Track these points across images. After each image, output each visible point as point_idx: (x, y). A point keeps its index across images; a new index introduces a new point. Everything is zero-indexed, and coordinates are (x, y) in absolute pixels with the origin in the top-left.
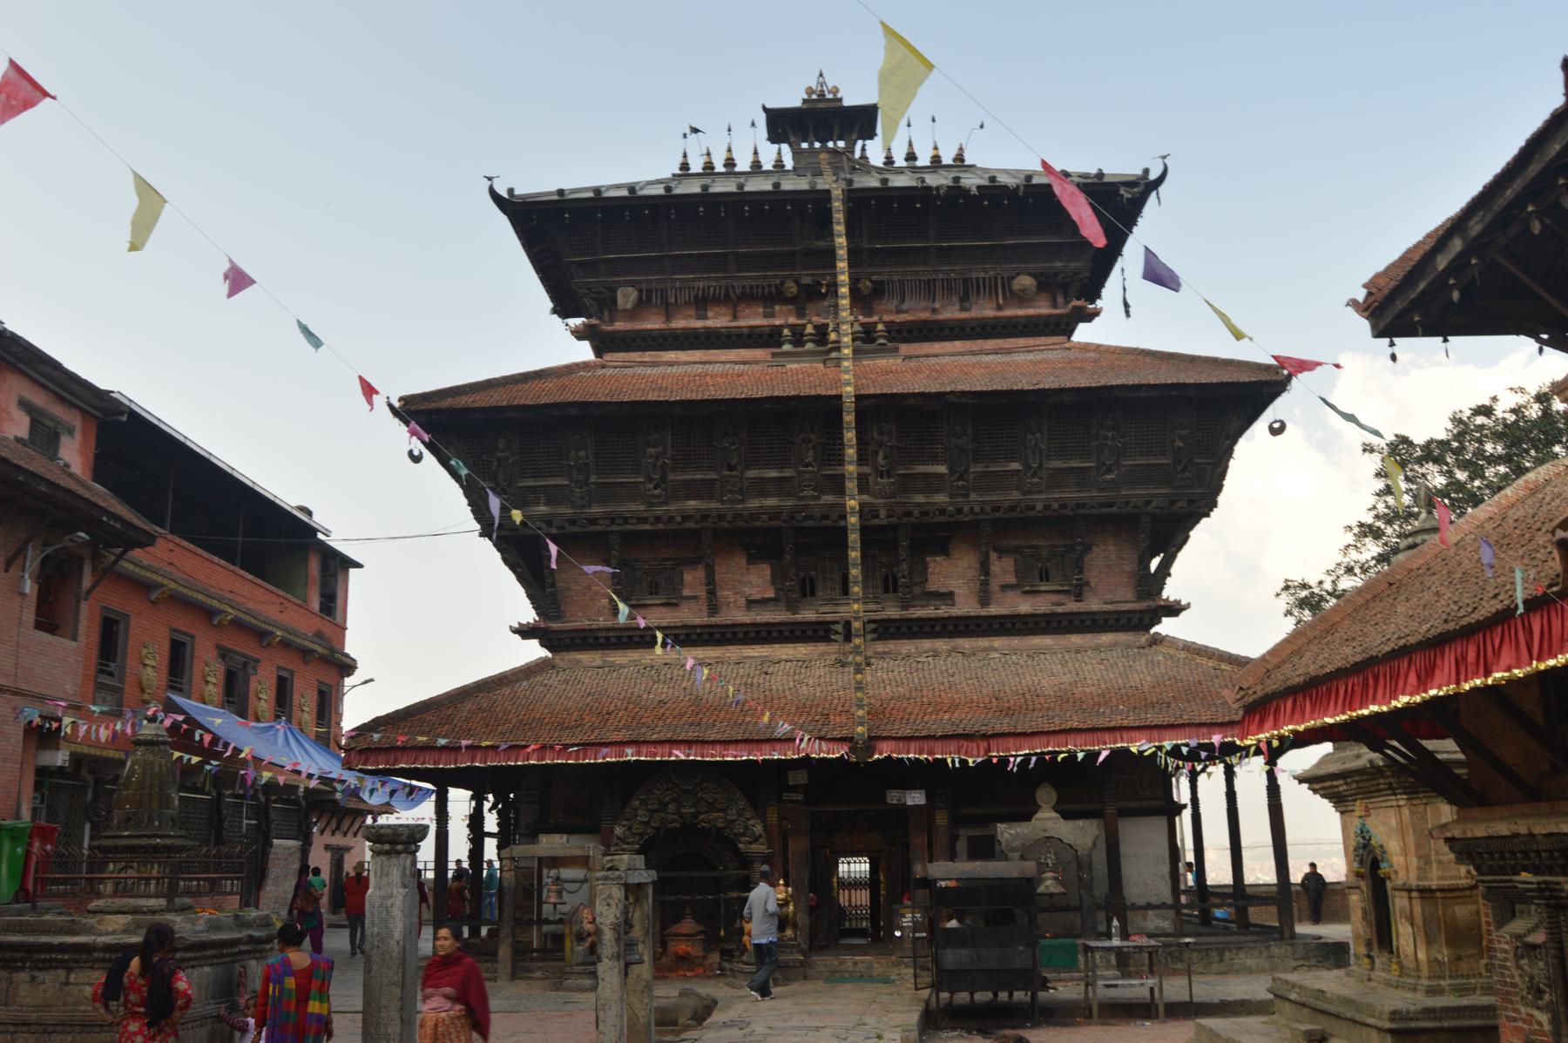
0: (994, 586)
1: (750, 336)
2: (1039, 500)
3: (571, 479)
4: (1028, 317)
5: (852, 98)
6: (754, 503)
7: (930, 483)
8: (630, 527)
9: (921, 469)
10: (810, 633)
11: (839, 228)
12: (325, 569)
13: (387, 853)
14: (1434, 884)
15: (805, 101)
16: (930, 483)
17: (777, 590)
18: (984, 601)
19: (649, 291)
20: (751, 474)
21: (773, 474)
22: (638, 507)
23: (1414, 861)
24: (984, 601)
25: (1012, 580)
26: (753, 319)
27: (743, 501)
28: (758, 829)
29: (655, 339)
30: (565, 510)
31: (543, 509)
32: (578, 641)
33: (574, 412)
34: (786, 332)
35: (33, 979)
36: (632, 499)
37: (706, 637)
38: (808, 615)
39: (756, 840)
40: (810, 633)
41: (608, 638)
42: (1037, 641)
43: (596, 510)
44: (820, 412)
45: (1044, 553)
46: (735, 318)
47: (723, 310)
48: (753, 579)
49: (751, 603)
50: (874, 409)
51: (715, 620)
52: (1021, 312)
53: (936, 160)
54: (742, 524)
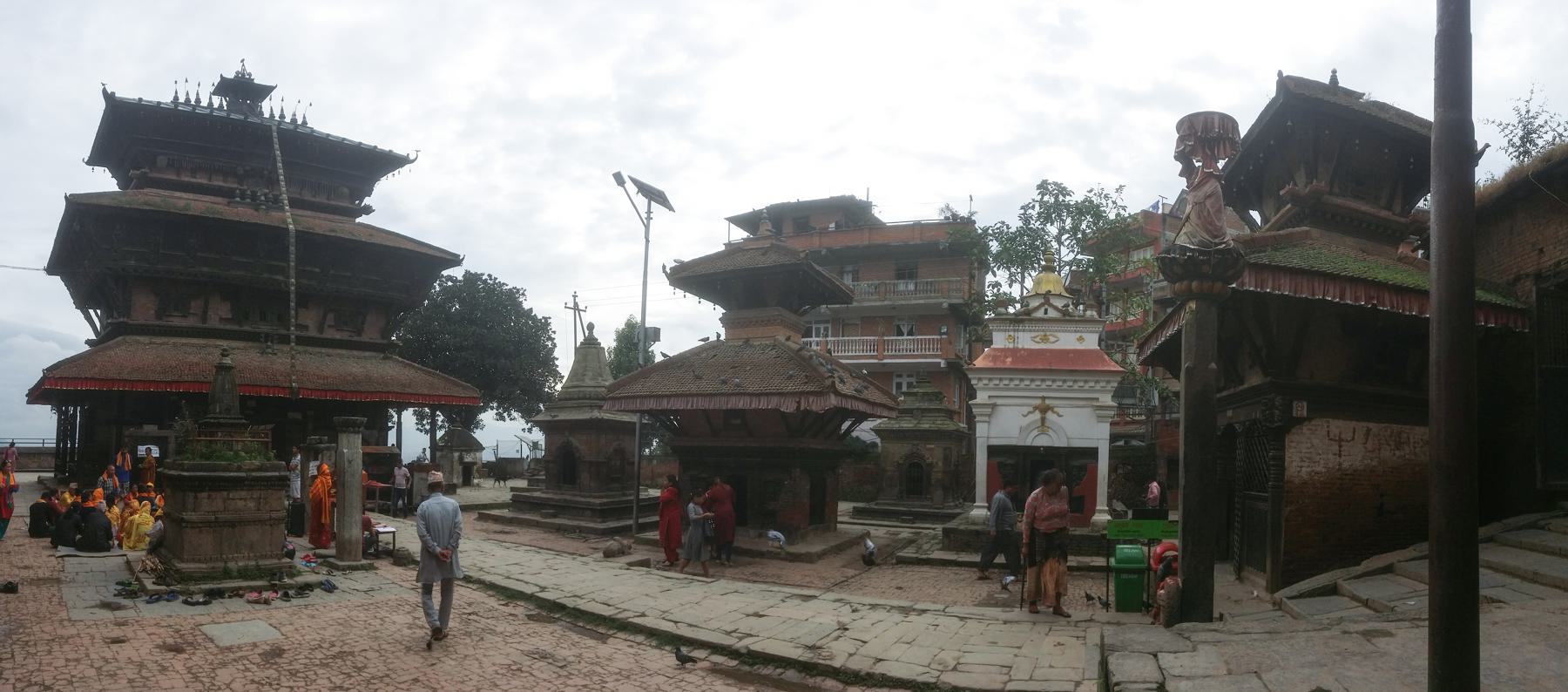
24: (321, 330)
26: (218, 182)
38: (246, 328)
50: (305, 237)
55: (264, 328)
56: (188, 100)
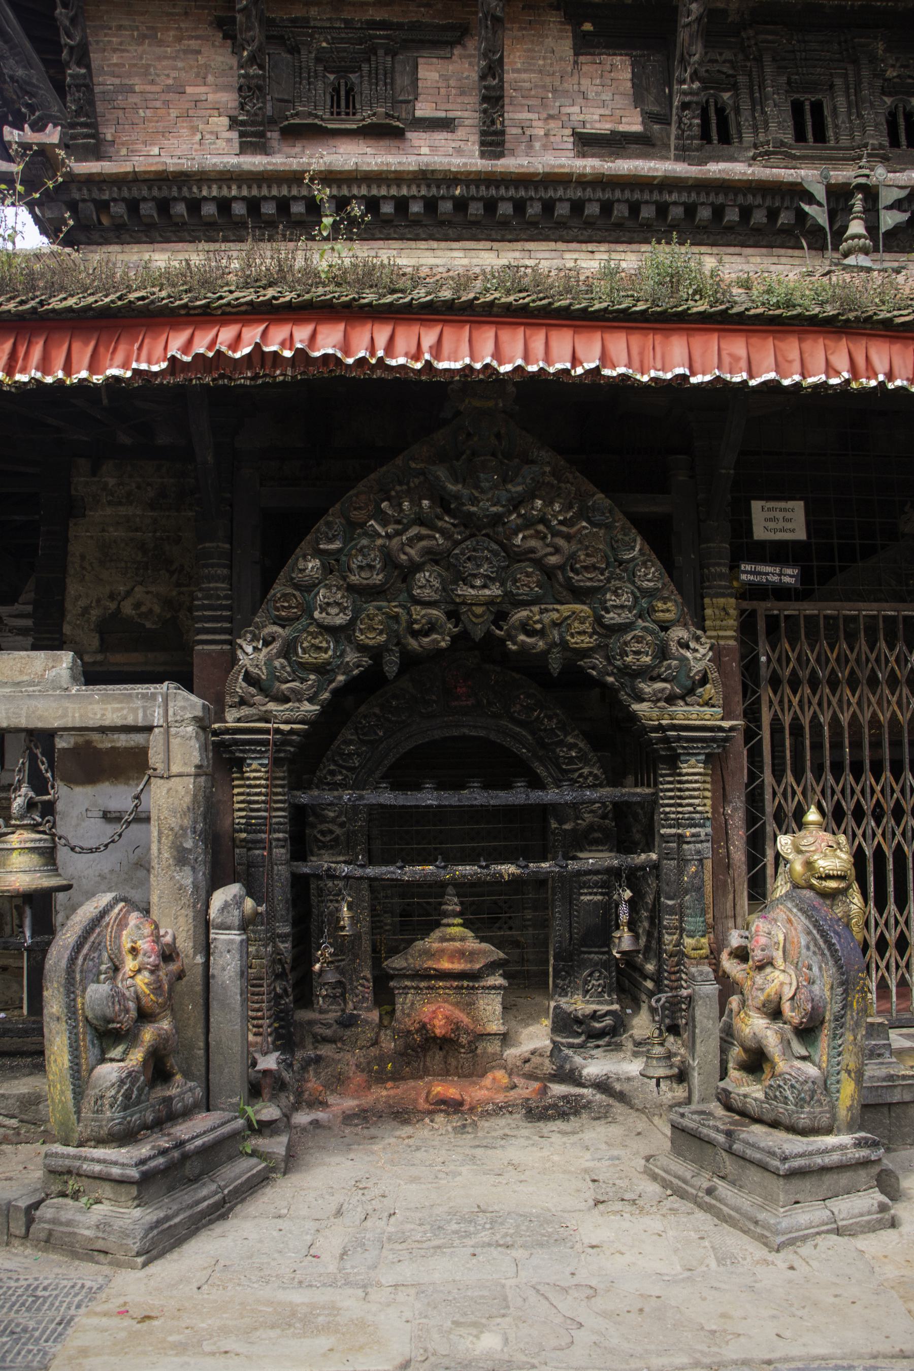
17: (649, 117)
28: (699, 657)
32: (147, 209)
37: (476, 209)
40: (732, 215)
49: (586, 143)
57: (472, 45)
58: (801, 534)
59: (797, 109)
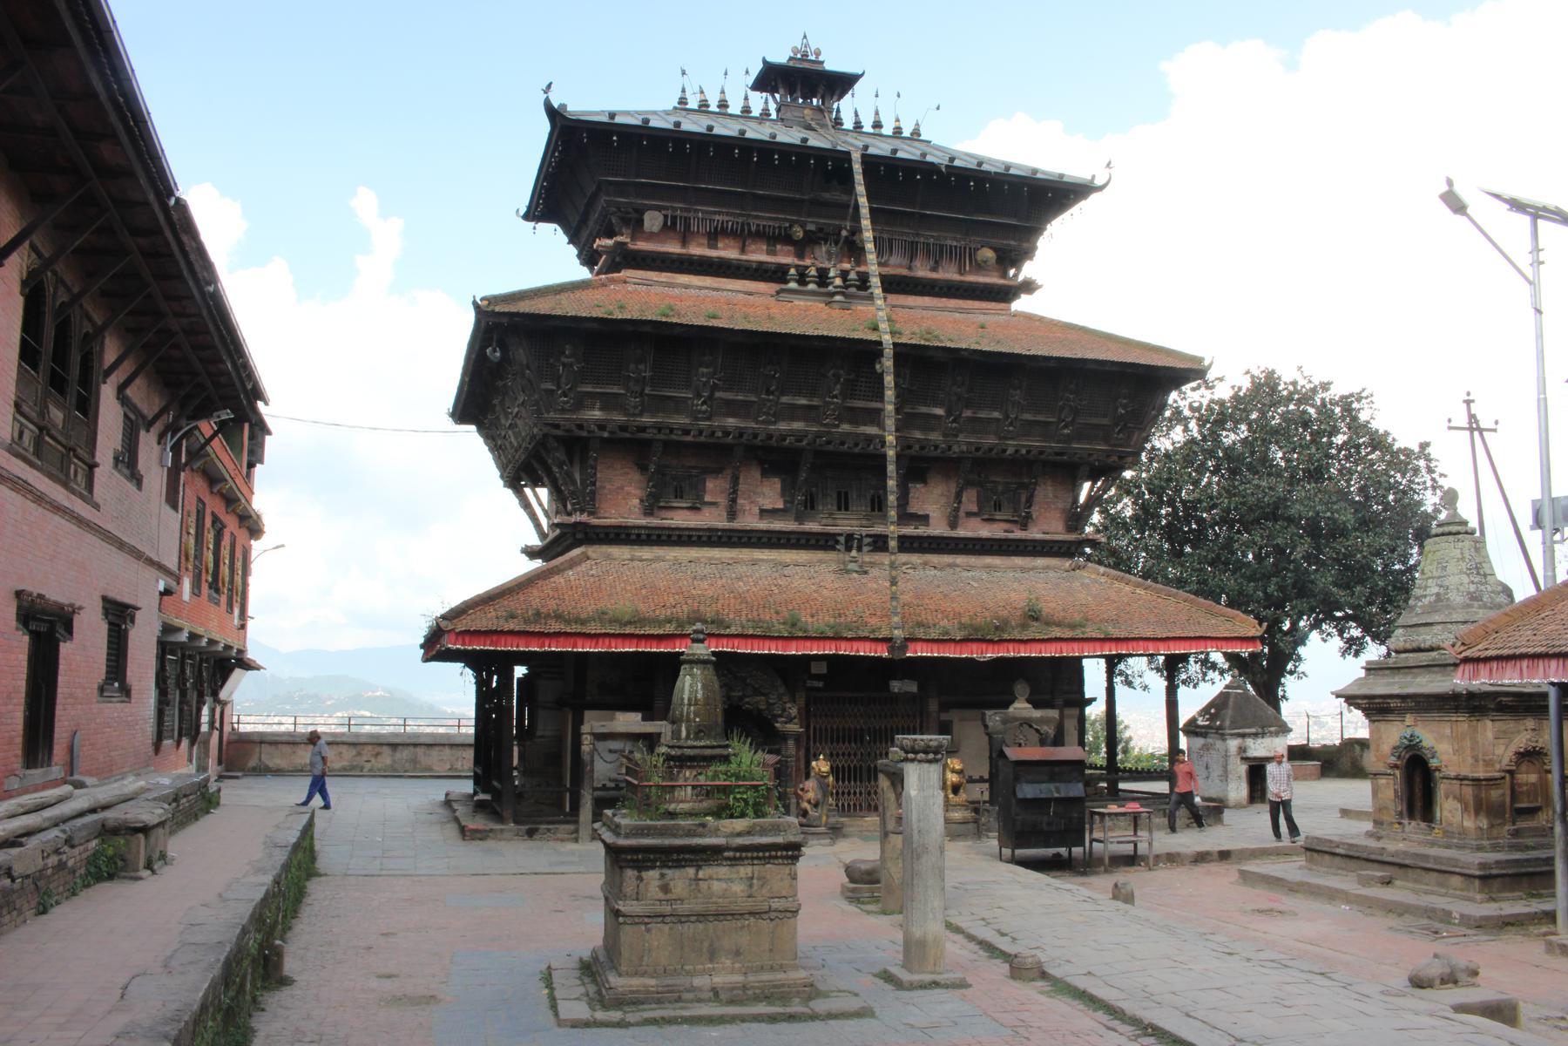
0: (962, 514)
1: (756, 270)
2: (1011, 446)
3: (628, 389)
4: (986, 285)
5: (832, 64)
6: (783, 426)
7: (928, 422)
8: (674, 437)
9: (924, 410)
10: (813, 542)
11: (860, 189)
12: (252, 437)
13: (930, 761)
14: (1481, 775)
15: (791, 59)
16: (928, 422)
18: (953, 525)
19: (674, 218)
20: (784, 399)
21: (803, 401)
22: (682, 420)
23: (1470, 760)
24: (953, 525)
25: (975, 509)
26: (758, 255)
27: (775, 423)
28: (794, 712)
29: (673, 261)
30: (619, 418)
31: (597, 414)
33: (647, 329)
34: (793, 271)
35: (663, 876)
36: (678, 412)
38: (812, 526)
39: (790, 720)
40: (813, 542)
41: (639, 535)
42: (988, 560)
43: (646, 420)
44: (858, 356)
45: (1000, 488)
46: (743, 251)
47: (732, 243)
48: (766, 490)
49: (764, 513)
50: (909, 356)
51: (736, 525)
52: (982, 279)
53: (898, 131)
54: (773, 442)
55: (846, 524)
56: (704, 105)
57: (728, 472)
58: (824, 671)
59: (839, 494)
